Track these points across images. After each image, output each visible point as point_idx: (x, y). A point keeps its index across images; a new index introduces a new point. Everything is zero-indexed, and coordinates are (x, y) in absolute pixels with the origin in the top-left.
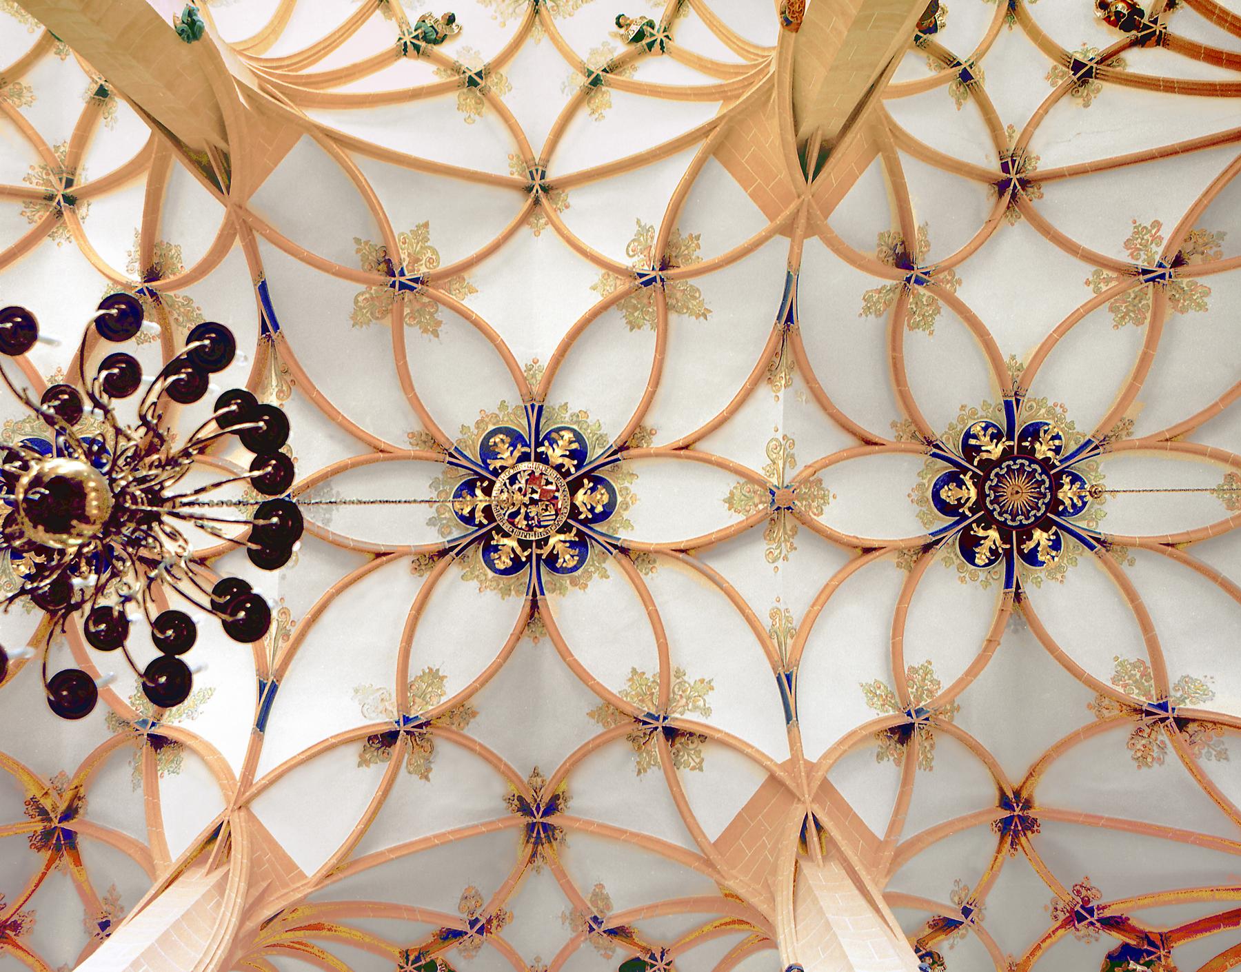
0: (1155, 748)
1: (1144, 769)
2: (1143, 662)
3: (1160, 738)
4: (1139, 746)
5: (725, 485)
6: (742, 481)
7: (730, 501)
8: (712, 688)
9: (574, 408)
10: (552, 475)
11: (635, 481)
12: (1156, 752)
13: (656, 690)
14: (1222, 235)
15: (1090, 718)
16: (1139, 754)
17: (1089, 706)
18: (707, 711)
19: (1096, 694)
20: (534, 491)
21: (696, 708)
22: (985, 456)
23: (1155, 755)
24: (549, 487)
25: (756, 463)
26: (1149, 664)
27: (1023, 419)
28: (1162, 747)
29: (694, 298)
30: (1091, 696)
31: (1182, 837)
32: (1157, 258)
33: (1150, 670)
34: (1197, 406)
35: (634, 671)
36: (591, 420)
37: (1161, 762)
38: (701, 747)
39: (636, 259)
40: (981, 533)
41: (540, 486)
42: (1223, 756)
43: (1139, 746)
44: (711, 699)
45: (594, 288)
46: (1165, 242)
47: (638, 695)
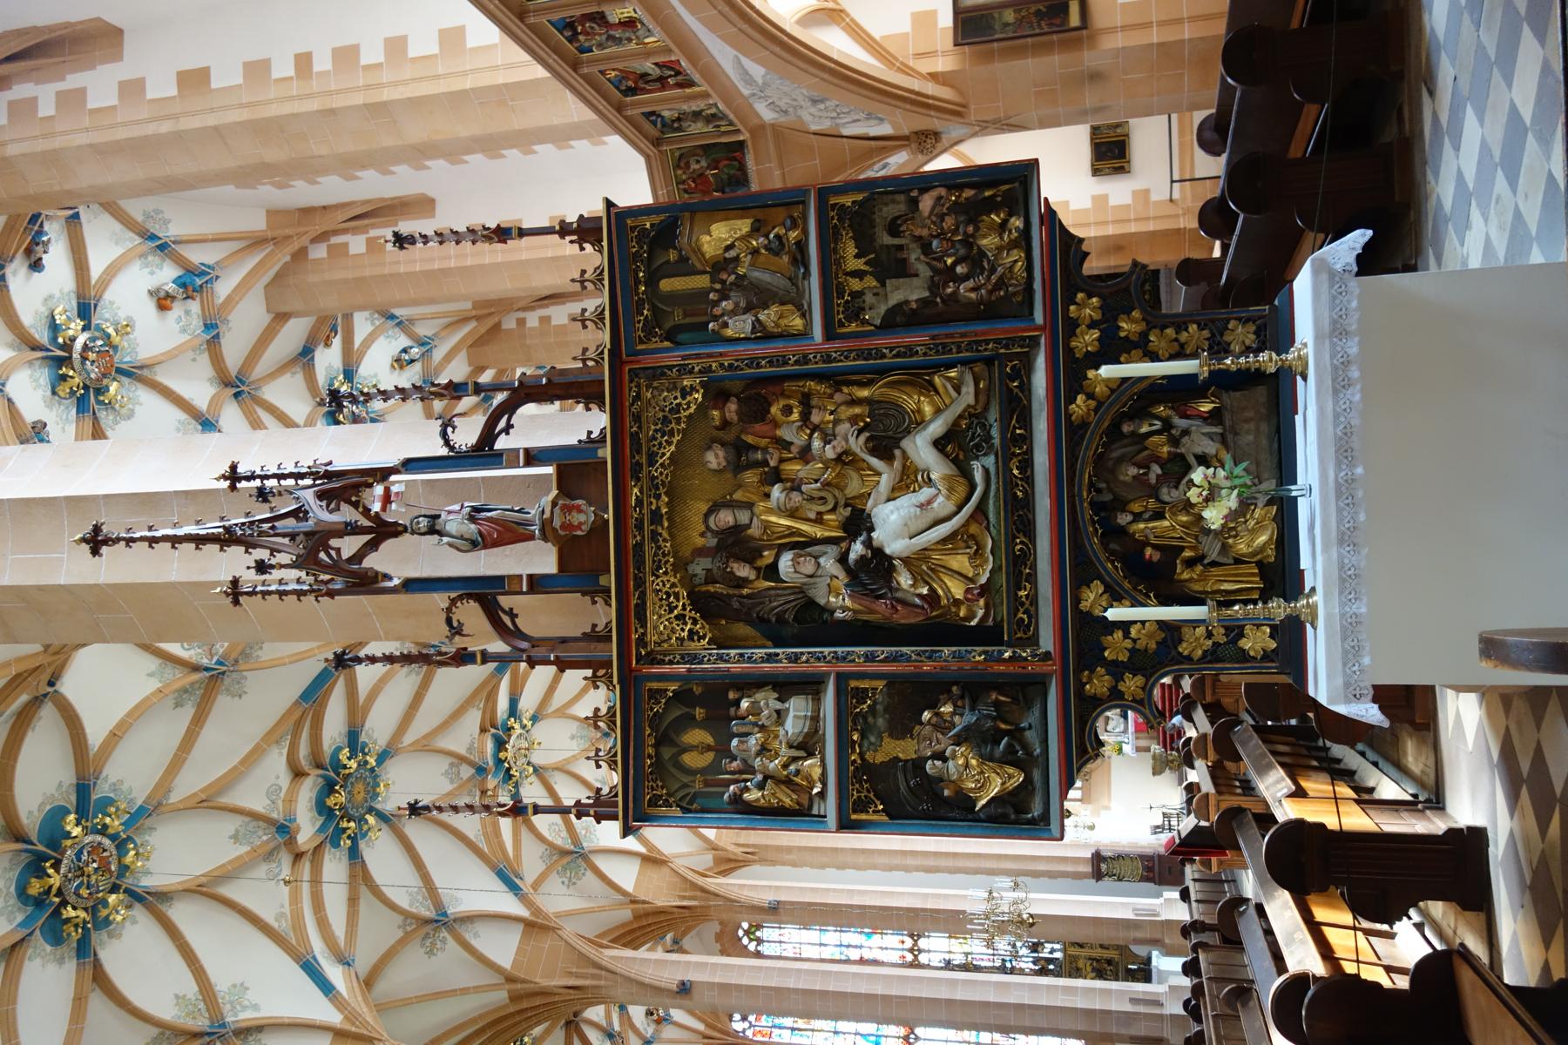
1: (433, 958)
5: (232, 824)
6: (247, 819)
7: (235, 837)
8: (247, 989)
9: (112, 780)
10: (107, 842)
11: (154, 833)
13: (202, 1005)
15: (400, 934)
17: (399, 927)
18: (255, 1007)
19: (402, 918)
20: (94, 861)
21: (245, 1008)
22: (347, 771)
24: (105, 854)
25: (259, 805)
27: (363, 738)
28: (444, 941)
29: (239, 683)
30: (399, 919)
31: (464, 991)
35: (177, 996)
36: (125, 787)
37: (443, 950)
38: (260, 1036)
39: (192, 652)
40: (344, 824)
41: (98, 855)
42: (476, 935)
44: (251, 996)
45: (150, 675)
47: (188, 1014)
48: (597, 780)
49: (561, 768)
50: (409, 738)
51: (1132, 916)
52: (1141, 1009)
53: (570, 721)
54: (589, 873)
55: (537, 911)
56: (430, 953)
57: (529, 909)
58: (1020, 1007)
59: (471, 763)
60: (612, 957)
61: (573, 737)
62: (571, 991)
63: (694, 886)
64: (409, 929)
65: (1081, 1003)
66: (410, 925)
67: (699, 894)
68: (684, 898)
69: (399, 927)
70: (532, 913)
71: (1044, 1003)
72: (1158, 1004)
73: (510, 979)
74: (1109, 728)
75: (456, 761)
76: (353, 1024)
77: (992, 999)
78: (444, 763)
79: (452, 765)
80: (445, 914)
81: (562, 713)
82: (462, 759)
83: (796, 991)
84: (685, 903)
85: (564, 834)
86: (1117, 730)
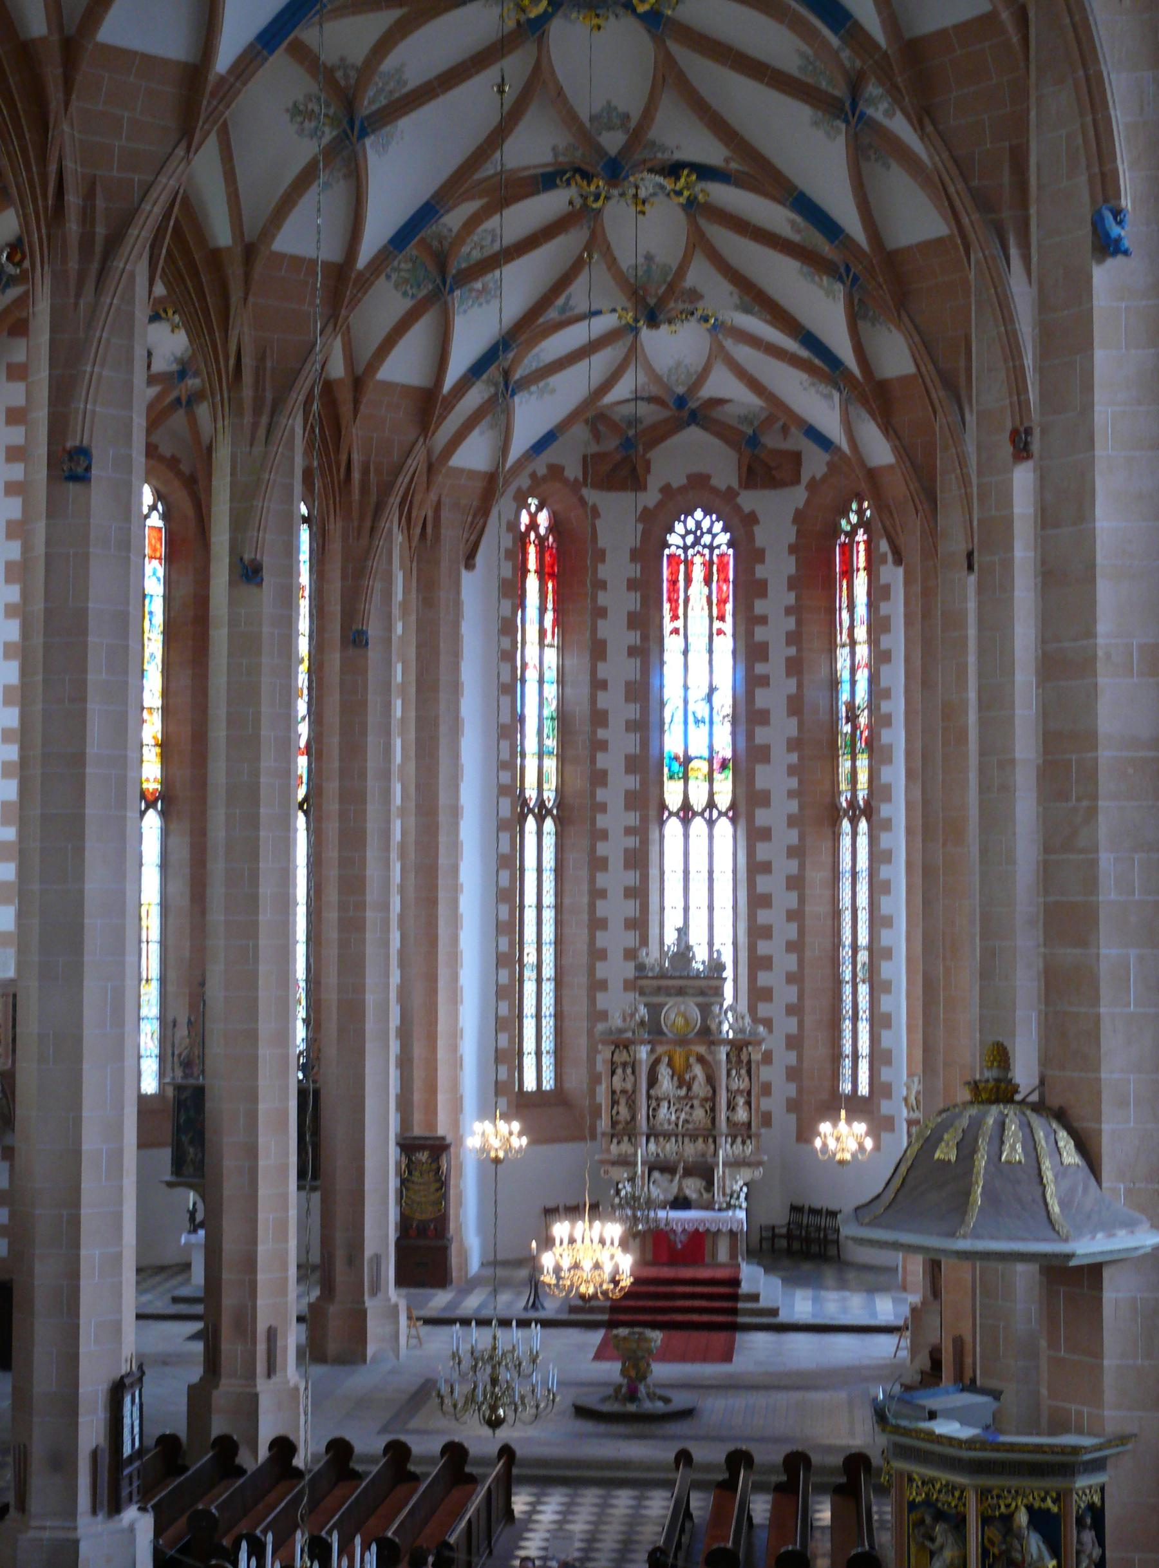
0: (313, 124)
1: (287, 117)
2: (406, 83)
3: (327, 130)
4: (310, 106)
12: (309, 125)
14: (888, 168)
16: (302, 107)
17: (342, 59)
23: (307, 124)
26: (405, 90)
28: (315, 134)
32: (870, 111)
33: (397, 95)
34: (705, 92)
37: (301, 132)
43: (310, 106)
46: (886, 122)
48: (568, 299)
49: (597, 242)
50: (677, 50)
51: (368, 1253)
52: (261, 1347)
53: (681, 255)
54: (408, 303)
55: (365, 282)
56: (296, 111)
57: (370, 264)
58: (252, 1152)
59: (627, 149)
60: (293, 430)
61: (649, 258)
62: (232, 362)
63: (386, 489)
64: (339, 74)
65: (264, 1249)
66: (346, 77)
67: (373, 498)
68: (365, 472)
69: (342, 59)
70: (360, 274)
71: (261, 1192)
72: (271, 1371)
73: (250, 252)
74: (656, 1175)
75: (633, 124)
76: (213, 95)
77: (262, 1107)
78: (631, 102)
79: (627, 116)
80: (363, 134)
81: (698, 243)
82: (637, 136)
83: (255, 774)
84: (356, 475)
85: (476, 255)
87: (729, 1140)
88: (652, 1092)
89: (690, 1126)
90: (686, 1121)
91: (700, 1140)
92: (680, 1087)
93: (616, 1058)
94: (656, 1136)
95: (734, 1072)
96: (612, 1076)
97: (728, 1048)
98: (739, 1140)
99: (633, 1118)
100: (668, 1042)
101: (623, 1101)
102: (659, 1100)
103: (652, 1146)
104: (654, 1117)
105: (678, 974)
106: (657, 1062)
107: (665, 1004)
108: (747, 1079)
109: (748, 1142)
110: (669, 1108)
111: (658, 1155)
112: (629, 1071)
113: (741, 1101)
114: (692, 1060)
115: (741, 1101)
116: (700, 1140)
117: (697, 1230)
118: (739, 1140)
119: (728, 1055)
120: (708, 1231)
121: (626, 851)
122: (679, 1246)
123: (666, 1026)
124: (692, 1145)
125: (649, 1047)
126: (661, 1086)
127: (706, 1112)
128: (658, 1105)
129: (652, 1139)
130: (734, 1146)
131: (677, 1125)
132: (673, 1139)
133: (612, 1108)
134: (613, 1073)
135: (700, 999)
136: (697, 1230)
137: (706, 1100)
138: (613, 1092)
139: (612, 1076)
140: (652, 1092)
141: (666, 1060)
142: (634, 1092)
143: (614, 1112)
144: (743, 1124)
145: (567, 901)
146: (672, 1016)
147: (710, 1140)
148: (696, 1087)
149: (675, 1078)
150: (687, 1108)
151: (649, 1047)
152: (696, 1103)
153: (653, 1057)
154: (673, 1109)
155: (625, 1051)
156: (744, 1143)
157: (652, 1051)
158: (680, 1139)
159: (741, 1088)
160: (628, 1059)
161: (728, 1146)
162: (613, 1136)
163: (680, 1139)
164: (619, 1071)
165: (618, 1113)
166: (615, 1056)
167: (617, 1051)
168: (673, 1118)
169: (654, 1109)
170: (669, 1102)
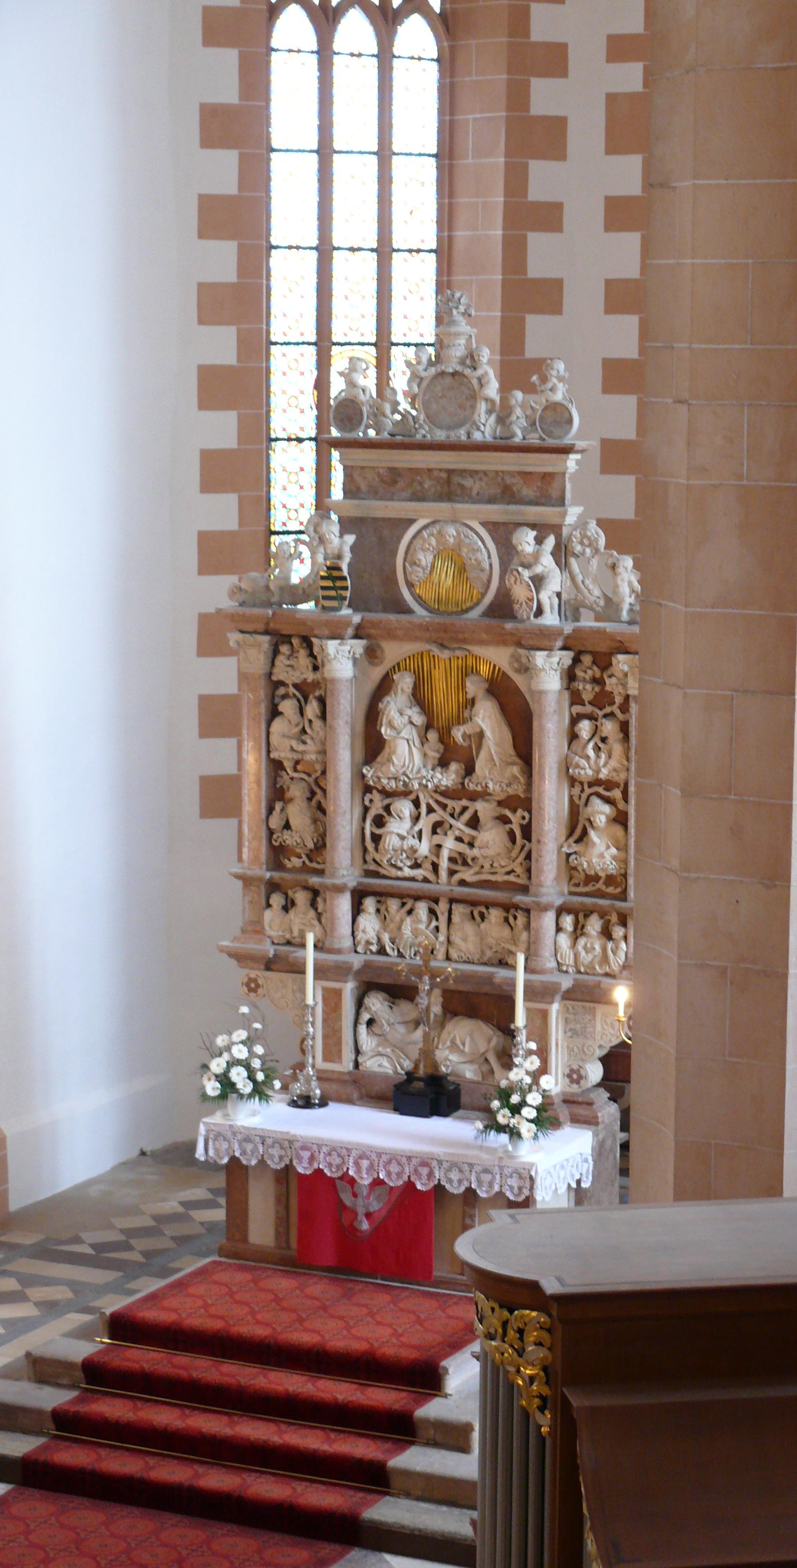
74: (376, 1003)
86: (367, 1041)
87: (568, 921)
88: (367, 771)
89: (468, 875)
90: (459, 860)
91: (495, 915)
92: (443, 763)
93: (280, 674)
94: (381, 895)
95: (585, 728)
96: (269, 724)
97: (567, 657)
98: (594, 925)
99: (321, 846)
100: (410, 634)
101: (297, 792)
102: (386, 794)
103: (369, 924)
104: (377, 839)
105: (440, 435)
106: (384, 687)
107: (411, 522)
108: (617, 749)
109: (618, 932)
110: (416, 819)
111: (382, 951)
112: (312, 709)
113: (601, 812)
114: (473, 687)
115: (601, 812)
116: (495, 915)
117: (410, 1185)
118: (594, 925)
119: (570, 676)
120: (439, 1188)
121: (612, 99)
122: (365, 1226)
123: (410, 585)
124: (469, 928)
125: (358, 646)
126: (390, 760)
127: (512, 836)
128: (387, 808)
129: (369, 904)
130: (582, 941)
131: (435, 867)
132: (422, 909)
133: (270, 810)
134: (274, 713)
135: (496, 512)
136: (410, 1185)
137: (510, 803)
138: (276, 766)
139: (269, 724)
140: (367, 771)
141: (405, 682)
142: (324, 773)
143: (275, 822)
144: (610, 880)
145: (461, 234)
146: (425, 559)
147: (521, 920)
148: (480, 765)
149: (432, 736)
150: (460, 825)
151: (358, 646)
152: (483, 809)
153: (377, 674)
154: (425, 823)
155: (303, 653)
156: (606, 933)
157: (372, 654)
158: (442, 908)
159: (604, 774)
160: (310, 676)
161: (564, 940)
162: (273, 887)
163: (442, 908)
164: (288, 707)
165: (287, 826)
166: (281, 660)
167: (284, 649)
168: (424, 848)
169: (379, 822)
170: (416, 803)
